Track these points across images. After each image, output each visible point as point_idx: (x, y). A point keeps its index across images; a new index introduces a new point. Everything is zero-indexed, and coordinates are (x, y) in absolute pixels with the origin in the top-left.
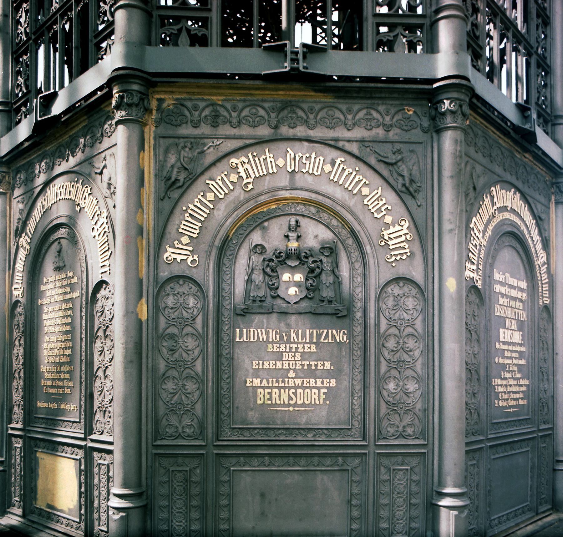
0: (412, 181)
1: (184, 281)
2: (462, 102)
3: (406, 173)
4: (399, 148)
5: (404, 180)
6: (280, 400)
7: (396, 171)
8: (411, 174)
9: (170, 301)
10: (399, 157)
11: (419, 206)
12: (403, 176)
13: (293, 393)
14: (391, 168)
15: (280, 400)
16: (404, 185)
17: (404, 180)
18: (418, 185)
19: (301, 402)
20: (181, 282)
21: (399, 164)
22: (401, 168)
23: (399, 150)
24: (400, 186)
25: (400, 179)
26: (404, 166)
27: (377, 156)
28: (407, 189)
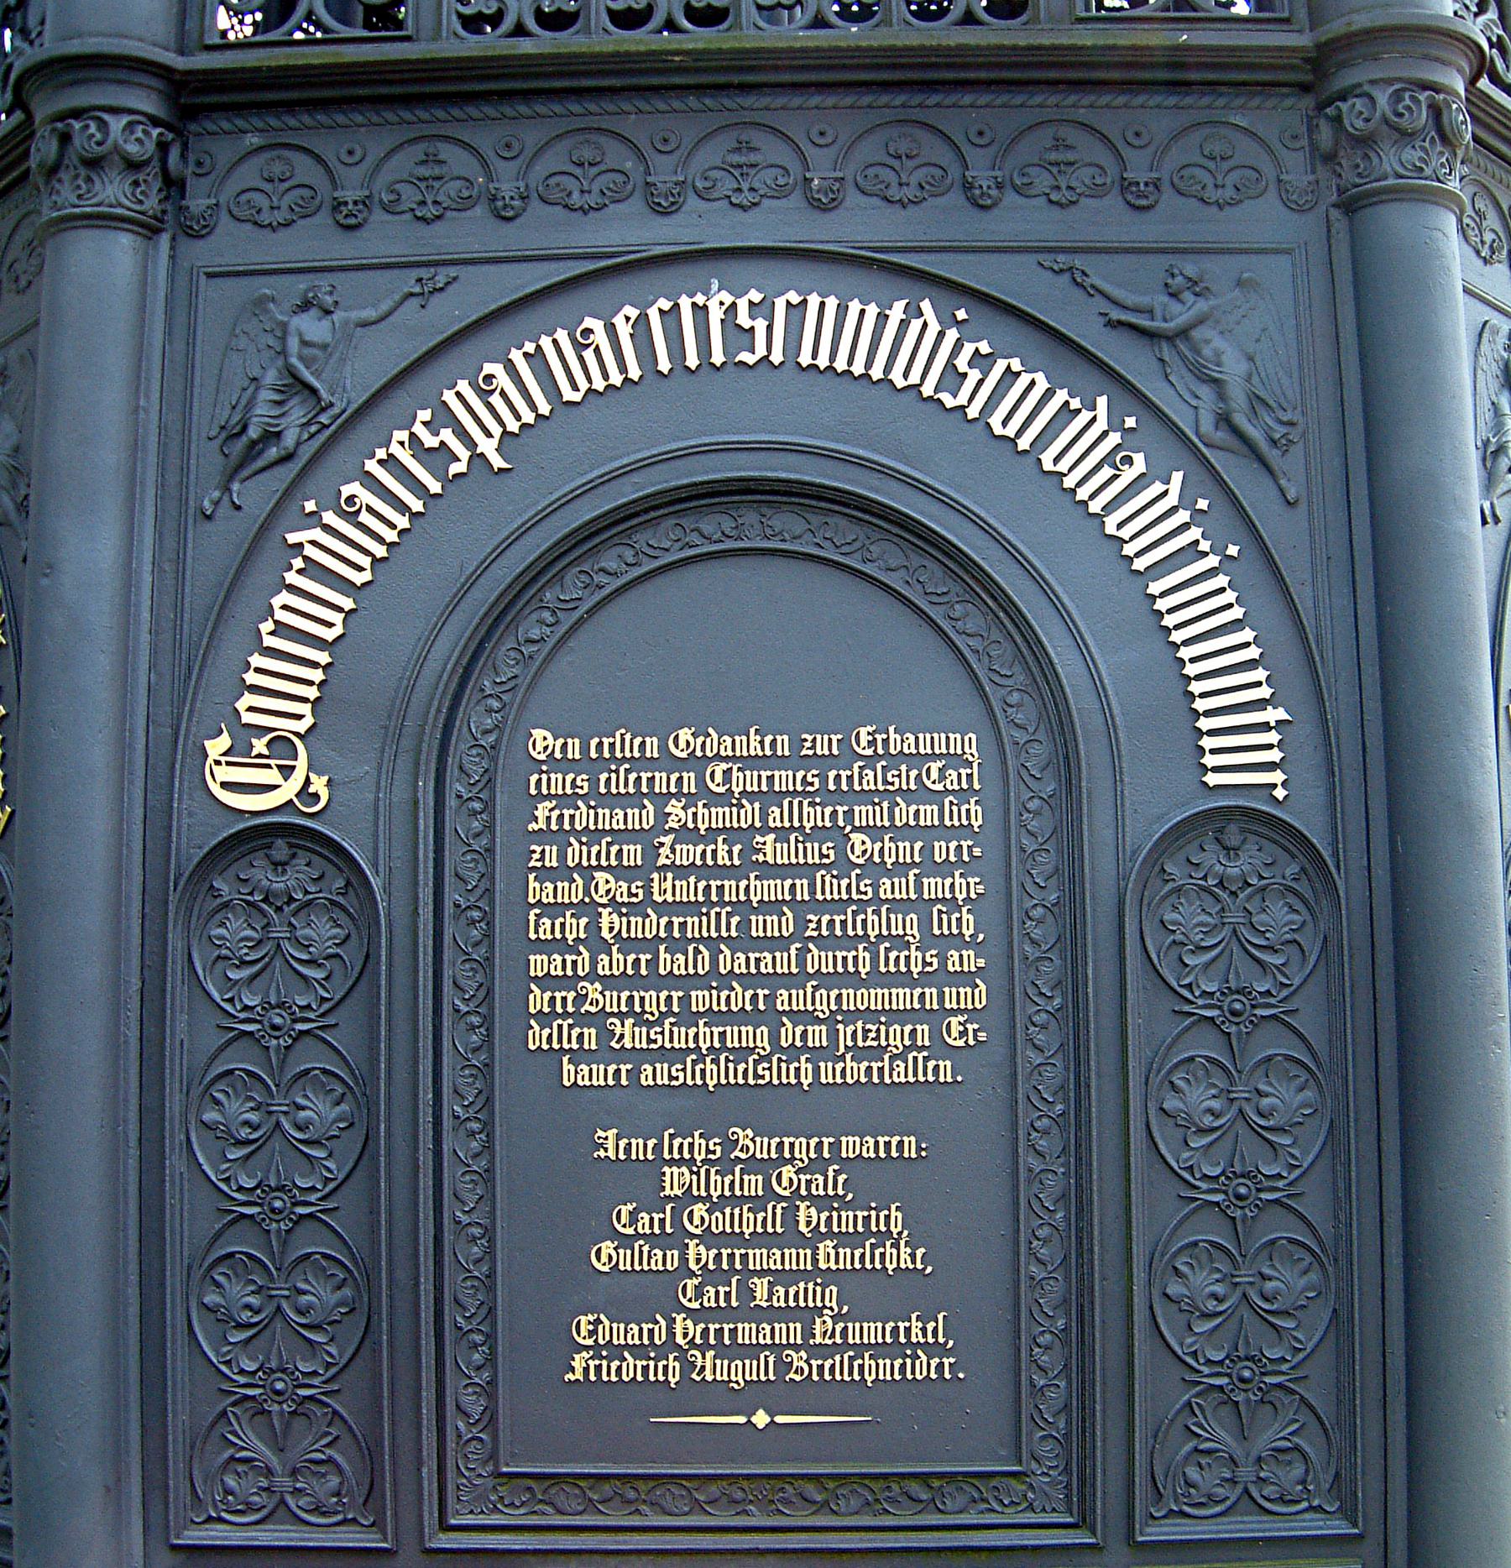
1: (291, 846)
4: (1190, 270)
5: (1222, 396)
8: (1249, 379)
9: (236, 930)
14: (1166, 352)
16: (1224, 420)
17: (1222, 396)
20: (281, 849)
21: (1196, 334)
22: (1207, 351)
24: (1207, 424)
25: (1205, 391)
26: (1218, 343)
27: (1105, 306)
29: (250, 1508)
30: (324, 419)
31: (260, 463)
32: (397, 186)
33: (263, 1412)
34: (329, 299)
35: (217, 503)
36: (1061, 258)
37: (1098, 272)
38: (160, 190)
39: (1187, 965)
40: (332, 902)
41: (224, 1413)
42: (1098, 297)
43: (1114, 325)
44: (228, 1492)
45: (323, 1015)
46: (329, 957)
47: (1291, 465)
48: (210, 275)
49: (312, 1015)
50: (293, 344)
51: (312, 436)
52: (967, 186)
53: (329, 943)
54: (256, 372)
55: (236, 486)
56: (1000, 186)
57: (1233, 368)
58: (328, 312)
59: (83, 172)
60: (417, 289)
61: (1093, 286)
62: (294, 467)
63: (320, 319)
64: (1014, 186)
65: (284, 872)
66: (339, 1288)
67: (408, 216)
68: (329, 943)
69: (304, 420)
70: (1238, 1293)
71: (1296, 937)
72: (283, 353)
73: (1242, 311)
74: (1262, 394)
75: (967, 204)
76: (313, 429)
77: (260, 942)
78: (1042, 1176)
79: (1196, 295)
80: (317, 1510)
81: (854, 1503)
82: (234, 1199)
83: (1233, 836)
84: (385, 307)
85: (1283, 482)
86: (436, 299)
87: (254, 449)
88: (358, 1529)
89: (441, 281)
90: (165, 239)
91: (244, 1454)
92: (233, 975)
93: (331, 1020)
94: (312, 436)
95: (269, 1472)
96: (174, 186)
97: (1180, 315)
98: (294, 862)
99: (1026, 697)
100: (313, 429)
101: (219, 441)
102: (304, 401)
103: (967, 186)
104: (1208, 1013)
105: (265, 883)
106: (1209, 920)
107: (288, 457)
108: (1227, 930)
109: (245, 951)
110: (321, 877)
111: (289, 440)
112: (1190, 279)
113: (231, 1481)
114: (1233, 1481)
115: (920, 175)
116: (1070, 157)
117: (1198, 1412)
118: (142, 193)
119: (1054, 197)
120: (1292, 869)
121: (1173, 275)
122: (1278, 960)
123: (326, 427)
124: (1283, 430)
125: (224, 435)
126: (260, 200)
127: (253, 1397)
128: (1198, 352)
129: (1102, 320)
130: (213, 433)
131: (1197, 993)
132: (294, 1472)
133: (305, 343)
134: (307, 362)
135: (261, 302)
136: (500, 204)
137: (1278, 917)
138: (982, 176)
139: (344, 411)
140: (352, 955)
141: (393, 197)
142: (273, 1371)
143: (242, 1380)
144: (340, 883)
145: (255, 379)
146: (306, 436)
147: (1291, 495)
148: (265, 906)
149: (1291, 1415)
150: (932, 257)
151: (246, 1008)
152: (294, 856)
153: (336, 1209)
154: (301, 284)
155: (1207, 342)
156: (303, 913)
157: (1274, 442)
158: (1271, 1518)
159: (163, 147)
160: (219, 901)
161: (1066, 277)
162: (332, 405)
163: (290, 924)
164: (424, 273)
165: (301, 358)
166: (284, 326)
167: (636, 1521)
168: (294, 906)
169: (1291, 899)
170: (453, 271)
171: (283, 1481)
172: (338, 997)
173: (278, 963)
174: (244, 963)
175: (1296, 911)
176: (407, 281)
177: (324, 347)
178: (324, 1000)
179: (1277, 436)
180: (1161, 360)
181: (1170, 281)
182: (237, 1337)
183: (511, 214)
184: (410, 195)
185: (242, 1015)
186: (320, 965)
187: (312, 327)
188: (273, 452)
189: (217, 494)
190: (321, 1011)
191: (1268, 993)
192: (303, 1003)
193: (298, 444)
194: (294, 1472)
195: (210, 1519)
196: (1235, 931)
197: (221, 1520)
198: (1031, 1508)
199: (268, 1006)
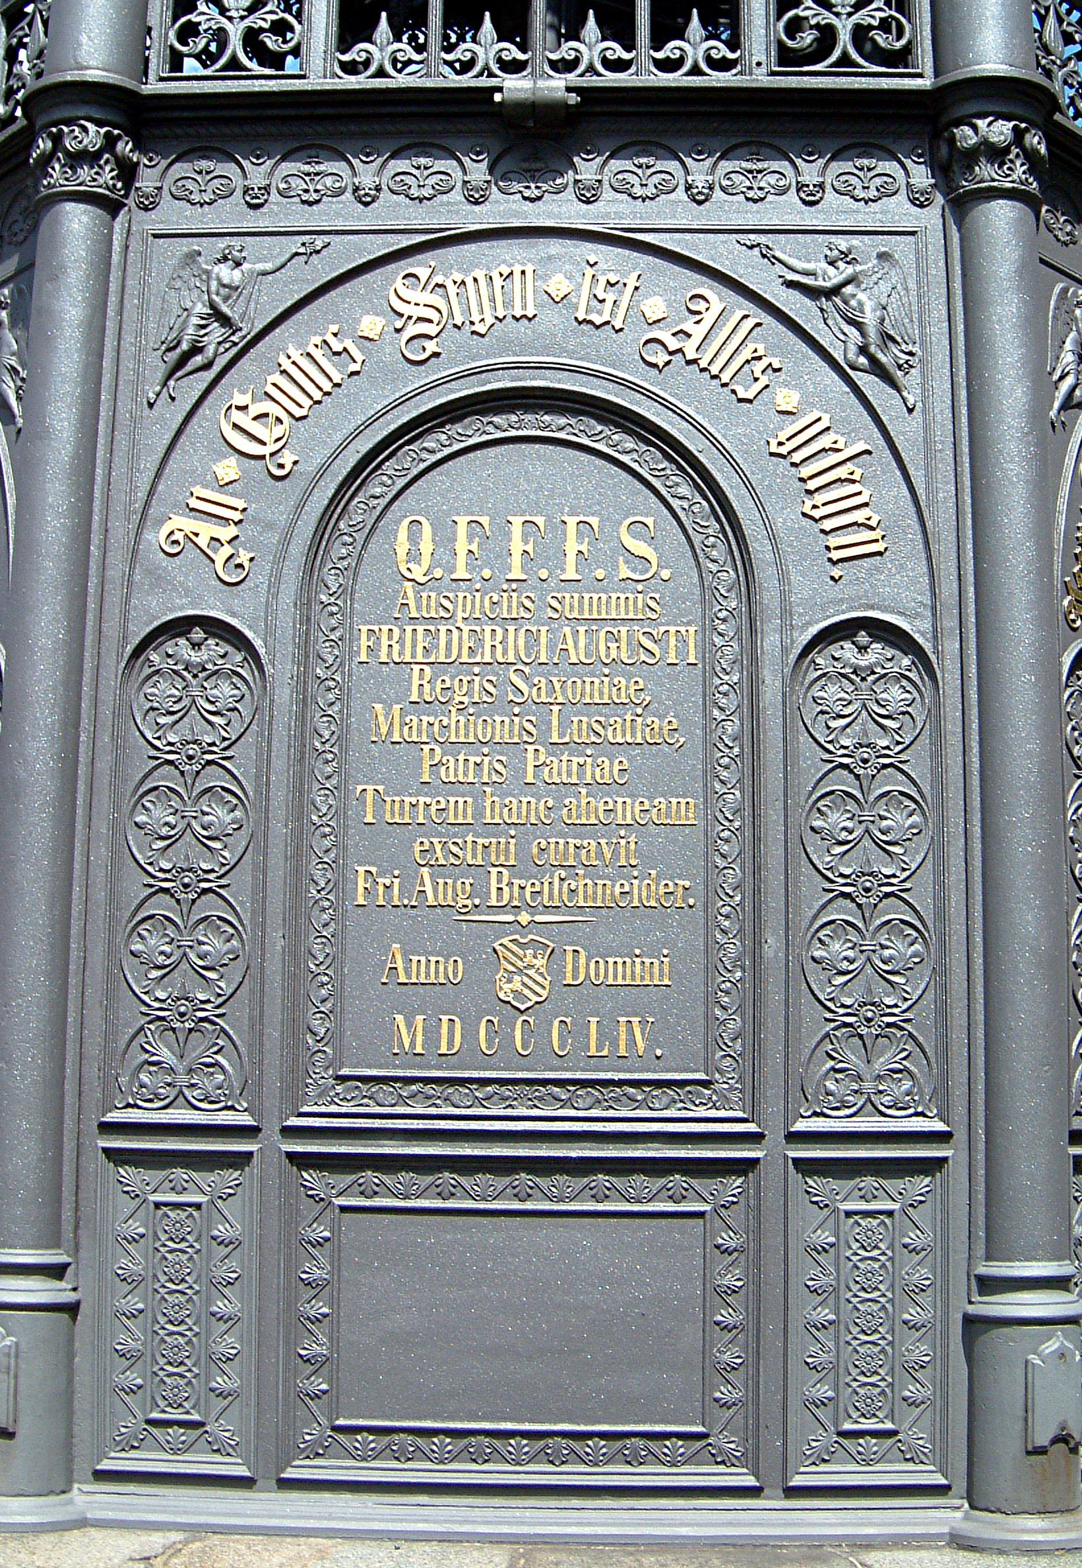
3: (870, 318)
5: (863, 334)
7: (838, 309)
9: (164, 690)
10: (850, 270)
11: (910, 411)
12: (859, 326)
16: (863, 350)
17: (863, 334)
21: (848, 290)
22: (853, 303)
24: (852, 351)
25: (852, 332)
26: (862, 296)
28: (873, 359)
32: (289, 179)
35: (158, 395)
36: (752, 236)
37: (781, 247)
39: (828, 727)
43: (790, 284)
44: (142, 1086)
46: (229, 710)
47: (911, 381)
48: (155, 236)
50: (214, 285)
53: (231, 700)
54: (189, 305)
55: (172, 383)
58: (238, 264)
60: (302, 250)
61: (774, 257)
62: (216, 368)
64: (723, 189)
66: (229, 941)
67: (297, 199)
69: (221, 339)
70: (863, 957)
71: (909, 709)
74: (892, 333)
75: (686, 199)
76: (227, 345)
78: (726, 871)
84: (278, 263)
85: (905, 394)
89: (319, 244)
91: (155, 1058)
92: (162, 720)
94: (227, 350)
97: (834, 277)
100: (227, 345)
101: (160, 353)
103: (688, 187)
104: (846, 760)
106: (847, 696)
107: (207, 366)
108: (856, 705)
112: (842, 253)
113: (144, 1077)
117: (835, 1041)
119: (750, 194)
121: (831, 249)
122: (892, 724)
123: (235, 344)
124: (907, 357)
125: (163, 348)
126: (190, 185)
130: (156, 346)
134: (226, 299)
137: (895, 695)
143: (157, 1005)
144: (239, 658)
145: (186, 310)
146: (222, 350)
147: (911, 401)
149: (902, 1046)
153: (228, 885)
154: (222, 243)
158: (882, 1119)
160: (153, 669)
161: (757, 249)
162: (241, 329)
163: (203, 686)
164: (306, 238)
167: (433, 1111)
169: (904, 683)
170: (327, 239)
171: (182, 1079)
172: (234, 738)
173: (194, 712)
175: (908, 692)
178: (225, 739)
179: (901, 362)
181: (828, 253)
182: (155, 974)
183: (369, 199)
185: (168, 748)
187: (225, 272)
188: (198, 360)
191: (888, 748)
192: (209, 741)
193: (216, 355)
195: (128, 1106)
198: (714, 1107)
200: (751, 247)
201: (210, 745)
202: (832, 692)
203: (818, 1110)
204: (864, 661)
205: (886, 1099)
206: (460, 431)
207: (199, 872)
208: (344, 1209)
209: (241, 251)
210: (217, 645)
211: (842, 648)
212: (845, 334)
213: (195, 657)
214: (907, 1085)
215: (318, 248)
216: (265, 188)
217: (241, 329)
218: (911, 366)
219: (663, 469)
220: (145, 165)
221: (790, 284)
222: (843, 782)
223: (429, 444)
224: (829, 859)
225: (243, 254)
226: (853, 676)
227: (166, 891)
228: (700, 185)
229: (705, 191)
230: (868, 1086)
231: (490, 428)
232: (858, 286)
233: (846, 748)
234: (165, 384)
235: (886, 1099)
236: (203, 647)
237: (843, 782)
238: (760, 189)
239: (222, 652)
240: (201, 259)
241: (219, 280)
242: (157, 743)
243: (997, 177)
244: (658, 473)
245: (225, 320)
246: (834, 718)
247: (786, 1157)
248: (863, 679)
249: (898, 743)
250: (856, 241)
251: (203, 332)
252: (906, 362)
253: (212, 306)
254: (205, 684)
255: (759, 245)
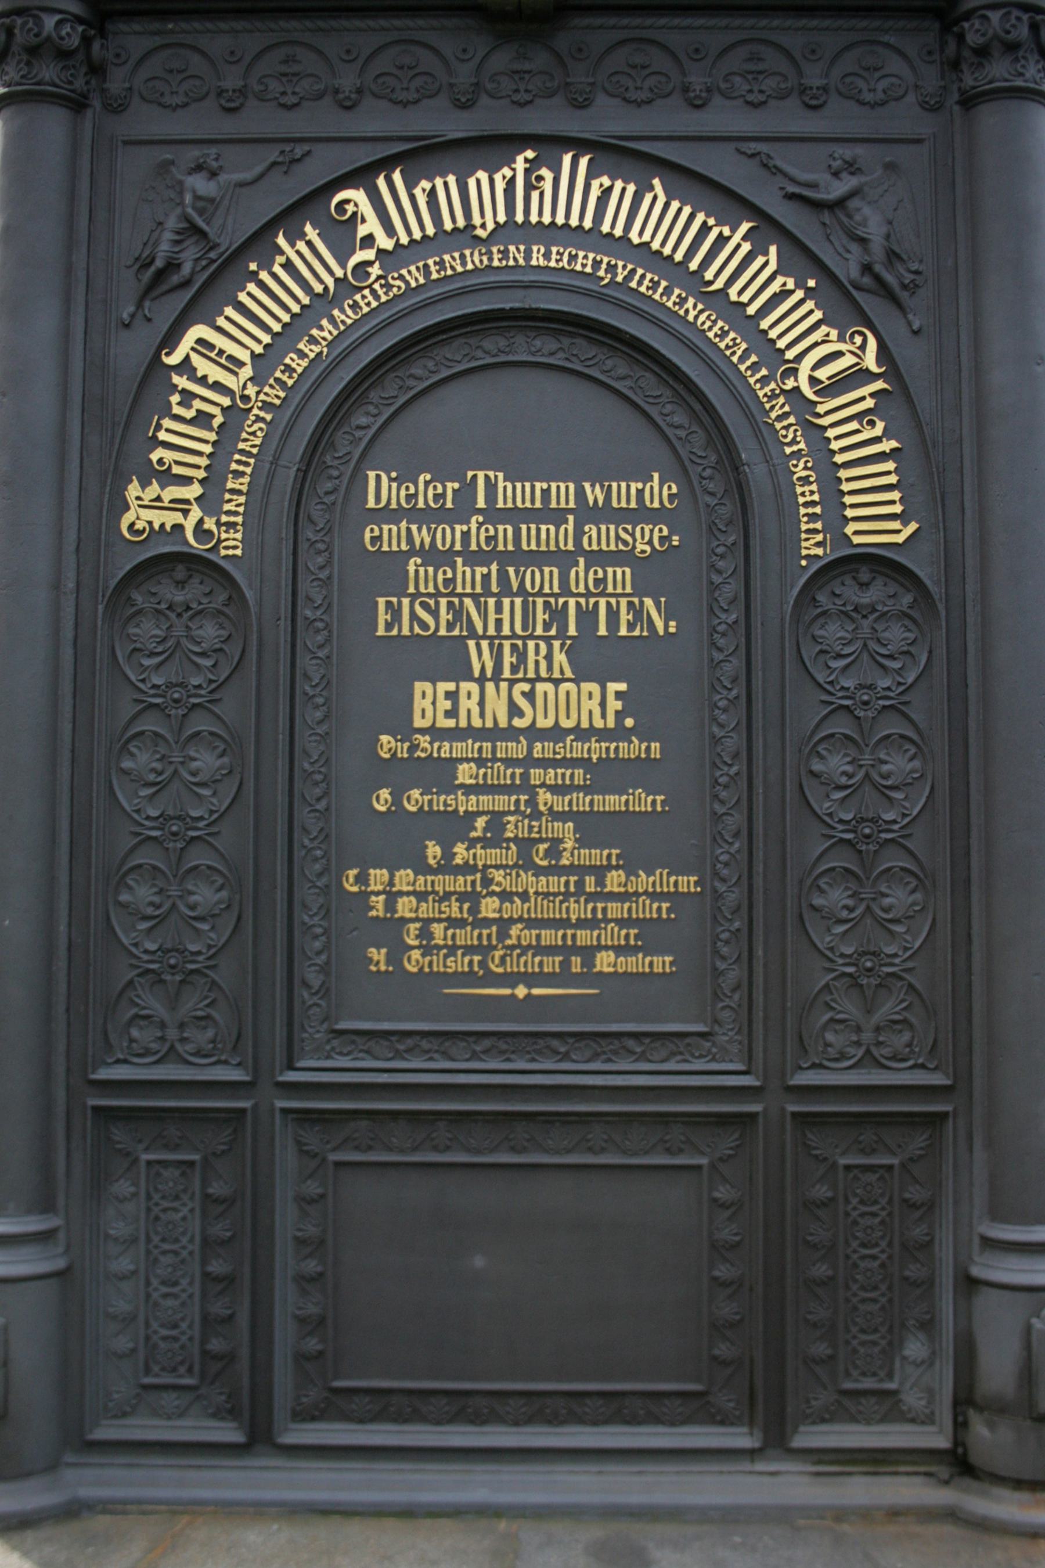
0: (892, 256)
1: (189, 569)
2: (1039, 17)
5: (867, 251)
6: (482, 715)
7: (841, 224)
8: (888, 237)
9: (148, 630)
12: (863, 241)
13: (523, 694)
14: (826, 217)
15: (482, 715)
16: (867, 269)
17: (867, 251)
18: (915, 267)
19: (549, 723)
20: (180, 571)
21: (853, 204)
22: (858, 218)
23: (850, 164)
24: (854, 272)
25: (854, 247)
26: (867, 210)
28: (878, 278)
29: (147, 1052)
30: (212, 255)
31: (165, 287)
32: (265, 80)
33: (162, 981)
34: (215, 164)
38: (86, 74)
40: (220, 612)
41: (131, 983)
42: (778, 174)
43: (791, 197)
44: (132, 1040)
45: (211, 692)
46: (215, 651)
48: (126, 143)
49: (203, 692)
50: (188, 198)
51: (204, 268)
52: (686, 89)
53: (216, 641)
55: (147, 304)
56: (709, 90)
57: (875, 229)
58: (213, 174)
59: (25, 57)
60: (280, 159)
61: (775, 167)
63: (210, 179)
65: (183, 588)
68: (216, 641)
69: (198, 255)
72: (181, 203)
73: (885, 187)
74: (898, 251)
77: (164, 640)
79: (852, 174)
80: (198, 1053)
81: (588, 1054)
82: (142, 825)
83: (864, 576)
85: (910, 317)
86: (297, 168)
87: (161, 275)
88: (230, 1067)
89: (299, 151)
90: (89, 113)
92: (146, 662)
93: (216, 696)
94: (204, 268)
95: (163, 1025)
96: (97, 70)
97: (837, 189)
98: (192, 581)
99: (716, 472)
100: (204, 263)
102: (197, 242)
103: (686, 89)
105: (169, 596)
106: (847, 635)
107: (186, 283)
108: (859, 644)
109: (154, 645)
110: (211, 592)
111: (186, 269)
112: (846, 162)
113: (135, 1033)
114: (858, 1044)
115: (651, 81)
116: (761, 67)
118: (71, 75)
120: (907, 599)
123: (214, 261)
124: (912, 277)
125: (136, 267)
127: (153, 971)
128: (850, 217)
129: (784, 193)
130: (129, 263)
131: (838, 688)
132: (182, 1026)
133: (197, 198)
134: (201, 212)
135: (165, 166)
136: (341, 96)
137: (896, 635)
138: (697, 81)
139: (227, 250)
140: (234, 650)
141: (262, 88)
142: (169, 951)
143: (145, 957)
144: (222, 597)
145: (160, 224)
146: (198, 268)
148: (167, 612)
150: (660, 144)
151: (154, 686)
152: (190, 577)
154: (194, 153)
155: (858, 210)
156: (198, 618)
157: (905, 287)
159: (86, 41)
162: (218, 245)
163: (187, 627)
164: (288, 148)
165: (194, 208)
166: (181, 183)
168: (190, 613)
169: (907, 622)
174: (152, 654)
175: (909, 630)
176: (272, 154)
177: (212, 200)
179: (907, 282)
180: (824, 224)
184: (274, 86)
185: (152, 692)
186: (209, 656)
187: (200, 184)
188: (175, 279)
189: (132, 309)
190: (209, 689)
191: (889, 689)
192: (196, 683)
193: (193, 273)
194: (182, 1026)
196: (865, 645)
197: (125, 1061)
198: (713, 1060)
199: (170, 685)
200: (752, 156)
201: (196, 687)
202: (833, 632)
203: (817, 1061)
204: (866, 598)
205: (886, 1051)
206: (448, 356)
207: (188, 820)
208: (338, 1164)
209: (217, 159)
210: (201, 583)
211: (843, 584)
212: (848, 251)
213: (179, 597)
214: (906, 1037)
215: (298, 156)
216: (240, 91)
217: (218, 245)
218: (917, 286)
219: (660, 396)
220: (112, 63)
221: (791, 197)
222: (842, 726)
223: (417, 371)
224: (829, 804)
225: (221, 163)
226: (854, 614)
227: (154, 839)
228: (698, 88)
229: (704, 95)
230: (867, 1036)
231: (479, 353)
232: (863, 199)
233: (848, 689)
234: (139, 305)
235: (886, 1051)
236: (186, 585)
237: (842, 726)
238: (761, 92)
239: (207, 591)
240: (173, 169)
241: (194, 191)
242: (141, 685)
243: (1011, 78)
244: (651, 400)
245: (203, 234)
246: (835, 658)
247: (783, 1109)
248: (865, 617)
249: (899, 684)
250: (860, 150)
251: (177, 249)
252: (912, 281)
253: (187, 219)
254: (190, 624)
255: (759, 153)
